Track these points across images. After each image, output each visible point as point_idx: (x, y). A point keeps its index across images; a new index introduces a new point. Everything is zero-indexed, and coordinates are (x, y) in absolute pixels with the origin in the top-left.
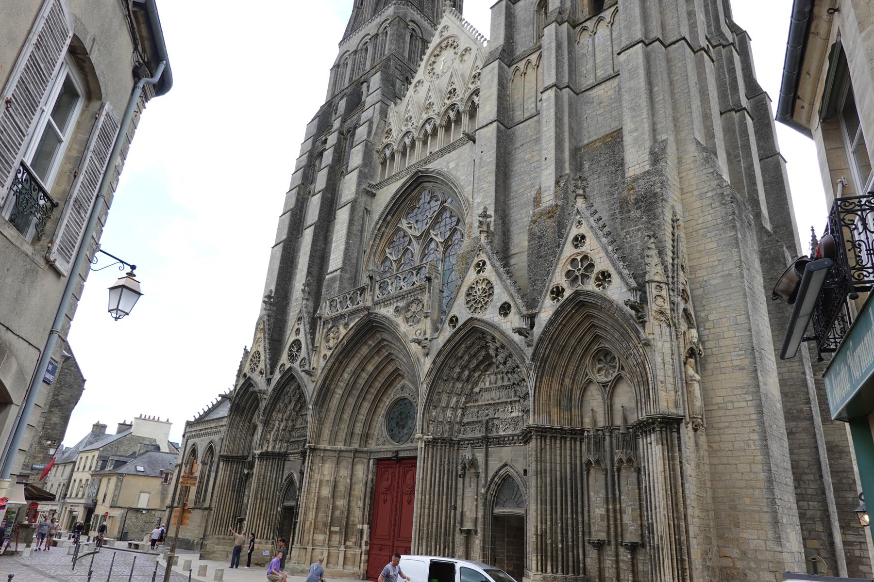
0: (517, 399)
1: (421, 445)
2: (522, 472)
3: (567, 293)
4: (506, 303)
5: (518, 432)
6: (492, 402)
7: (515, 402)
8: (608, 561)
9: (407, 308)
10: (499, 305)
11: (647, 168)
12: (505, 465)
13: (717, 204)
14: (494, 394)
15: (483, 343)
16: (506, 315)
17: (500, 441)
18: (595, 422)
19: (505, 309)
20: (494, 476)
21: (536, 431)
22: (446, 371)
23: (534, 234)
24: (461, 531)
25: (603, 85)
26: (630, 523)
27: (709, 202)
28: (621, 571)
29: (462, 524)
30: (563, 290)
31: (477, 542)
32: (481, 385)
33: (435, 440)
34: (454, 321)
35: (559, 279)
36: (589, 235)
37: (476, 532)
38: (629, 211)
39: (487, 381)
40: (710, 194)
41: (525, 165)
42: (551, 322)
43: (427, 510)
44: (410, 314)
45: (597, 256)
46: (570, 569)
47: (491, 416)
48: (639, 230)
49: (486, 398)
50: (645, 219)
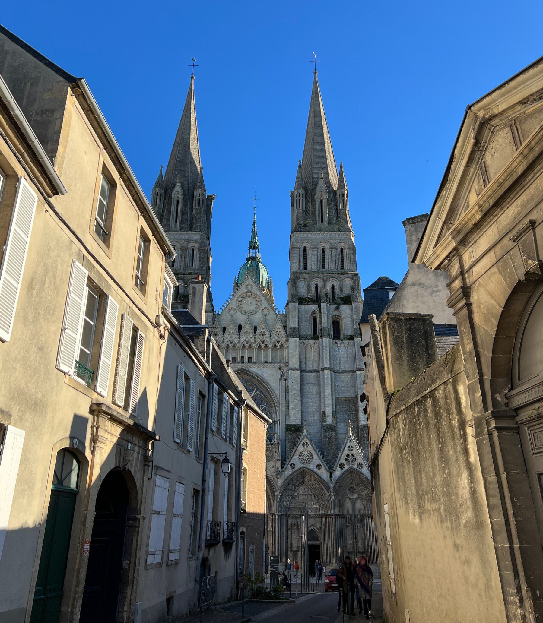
1: (277, 517)
3: (346, 467)
14: (305, 497)
16: (319, 469)
18: (348, 511)
23: (326, 436)
24: (291, 551)
25: (344, 374)
31: (299, 555)
32: (298, 492)
34: (293, 466)
35: (343, 461)
41: (309, 394)
42: (340, 477)
47: (304, 505)
49: (301, 498)
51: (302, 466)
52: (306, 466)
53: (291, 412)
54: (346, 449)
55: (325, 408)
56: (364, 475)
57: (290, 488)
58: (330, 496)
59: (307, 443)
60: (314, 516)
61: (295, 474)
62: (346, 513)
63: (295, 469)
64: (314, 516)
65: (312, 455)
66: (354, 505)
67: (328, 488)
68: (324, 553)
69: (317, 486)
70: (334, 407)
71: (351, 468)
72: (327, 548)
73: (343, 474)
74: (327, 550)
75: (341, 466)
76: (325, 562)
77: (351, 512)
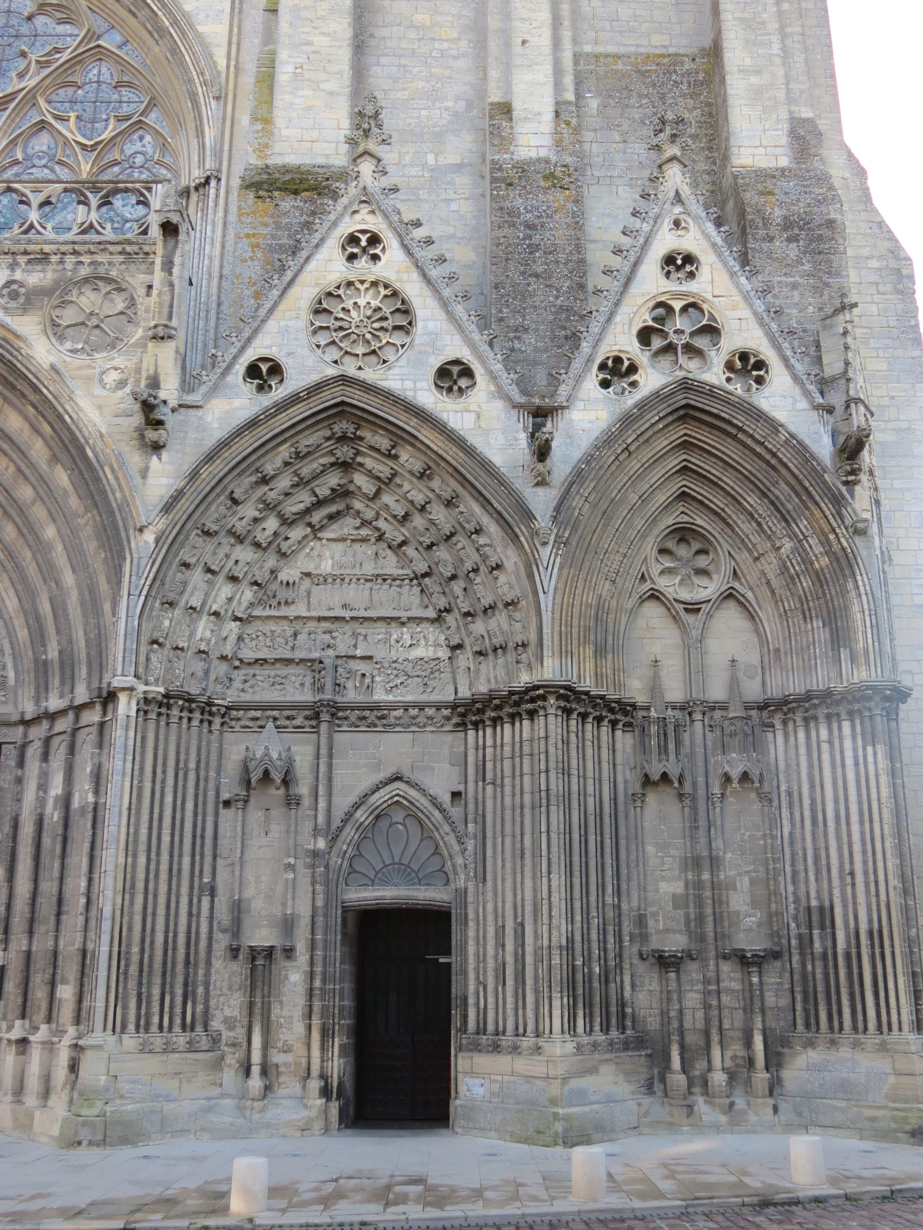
0: (431, 614)
2: (446, 798)
3: (652, 378)
4: (456, 362)
5: (436, 697)
6: (347, 614)
7: (419, 620)
8: (690, 995)
9: (59, 294)
10: (436, 362)
11: (784, 162)
12: (398, 778)
13: (889, 288)
15: (345, 452)
17: (375, 716)
18: (655, 687)
19: (453, 376)
20: (356, 806)
21: (559, 697)
22: (219, 506)
23: (512, 213)
24: (234, 952)
26: (744, 909)
27: (873, 278)
28: (726, 1013)
29: (236, 928)
30: (633, 369)
33: (167, 700)
34: (264, 373)
35: (622, 339)
36: (708, 260)
37: (289, 952)
38: (771, 239)
39: (325, 556)
40: (874, 264)
41: (412, 34)
42: (607, 440)
43: (139, 899)
44: (68, 316)
45: (731, 314)
46: (614, 1021)
47: (342, 650)
48: (794, 286)
49: (328, 600)
50: (807, 267)
51: (332, 371)
52: (370, 375)
53: (282, 98)
54: (651, 269)
55: (508, 90)
56: (774, 426)
57: (241, 527)
58: (530, 566)
59: (374, 240)
60: (413, 716)
61: (283, 421)
62: (641, 699)
63: (279, 392)
64: (413, 716)
65: (405, 310)
66: (693, 649)
67: (514, 519)
68: (481, 959)
69: (438, 513)
70: (569, 81)
71: (686, 385)
72: (500, 931)
73: (627, 420)
74: (501, 945)
75: (617, 371)
76: (481, 1030)
77: (675, 692)
